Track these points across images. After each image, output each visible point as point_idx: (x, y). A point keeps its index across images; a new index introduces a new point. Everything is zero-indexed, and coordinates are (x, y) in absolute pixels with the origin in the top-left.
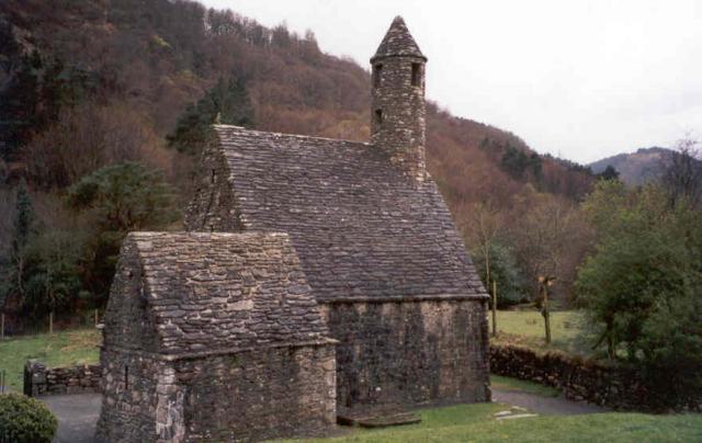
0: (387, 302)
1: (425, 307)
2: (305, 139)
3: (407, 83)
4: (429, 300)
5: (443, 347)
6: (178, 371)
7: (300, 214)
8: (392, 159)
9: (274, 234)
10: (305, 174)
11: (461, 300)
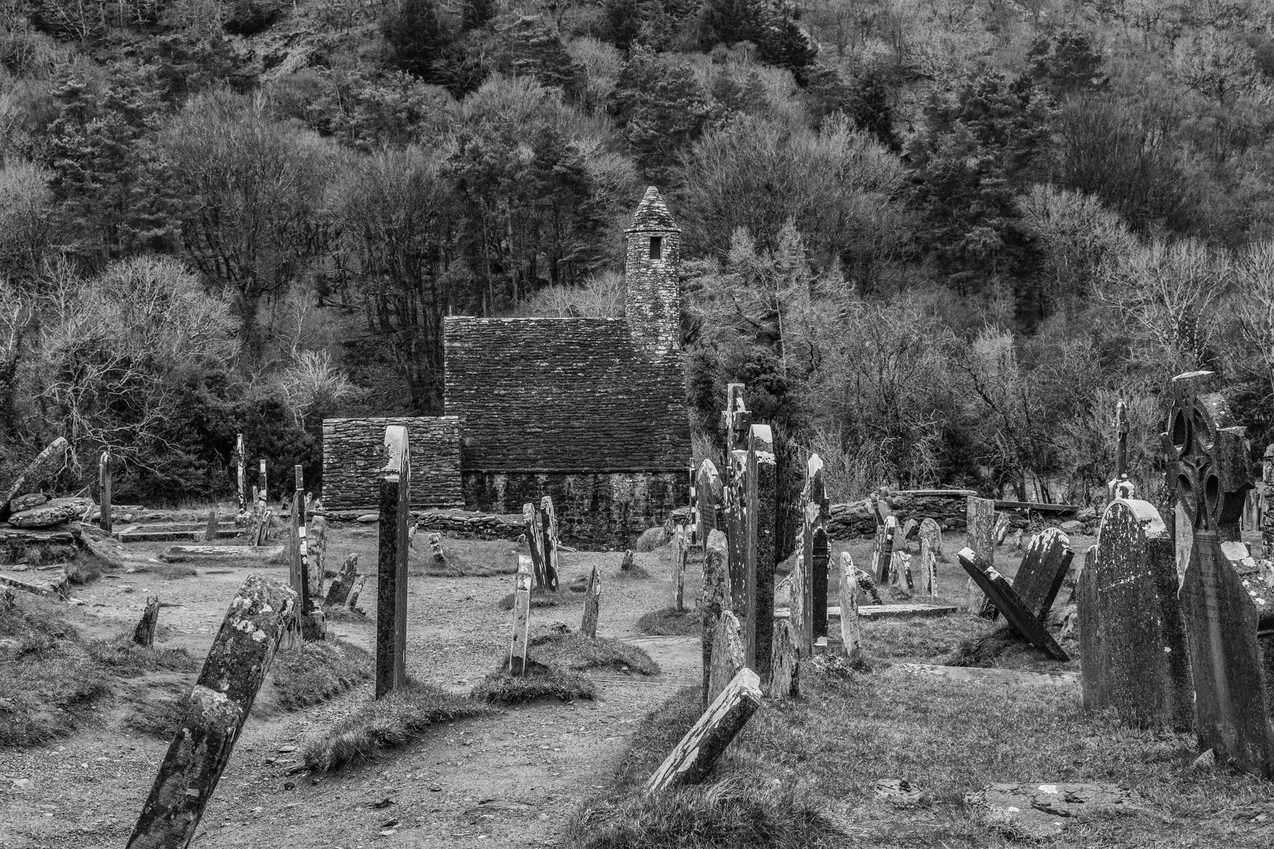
0: (569, 473)
1: (616, 477)
2: (537, 321)
3: (645, 258)
4: (620, 472)
5: (636, 514)
7: (504, 396)
8: (633, 333)
10: (522, 357)
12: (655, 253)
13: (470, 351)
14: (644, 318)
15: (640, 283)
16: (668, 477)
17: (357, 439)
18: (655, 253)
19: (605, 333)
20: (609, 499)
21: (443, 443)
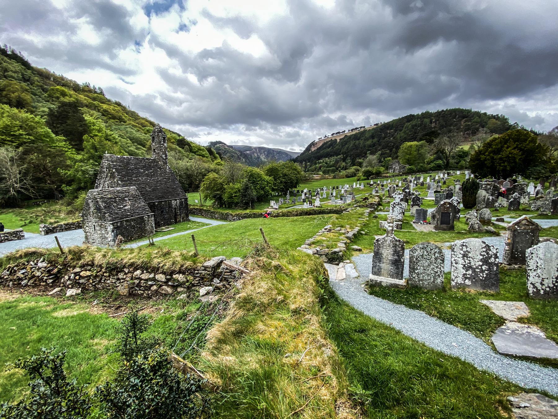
1: (173, 201)
3: (162, 142)
6: (113, 226)
9: (132, 187)
11: (181, 199)
12: (164, 142)
13: (120, 166)
14: (163, 159)
15: (161, 149)
16: (183, 200)
17: (109, 196)
18: (164, 142)
19: (152, 162)
20: (172, 207)
21: (137, 195)
